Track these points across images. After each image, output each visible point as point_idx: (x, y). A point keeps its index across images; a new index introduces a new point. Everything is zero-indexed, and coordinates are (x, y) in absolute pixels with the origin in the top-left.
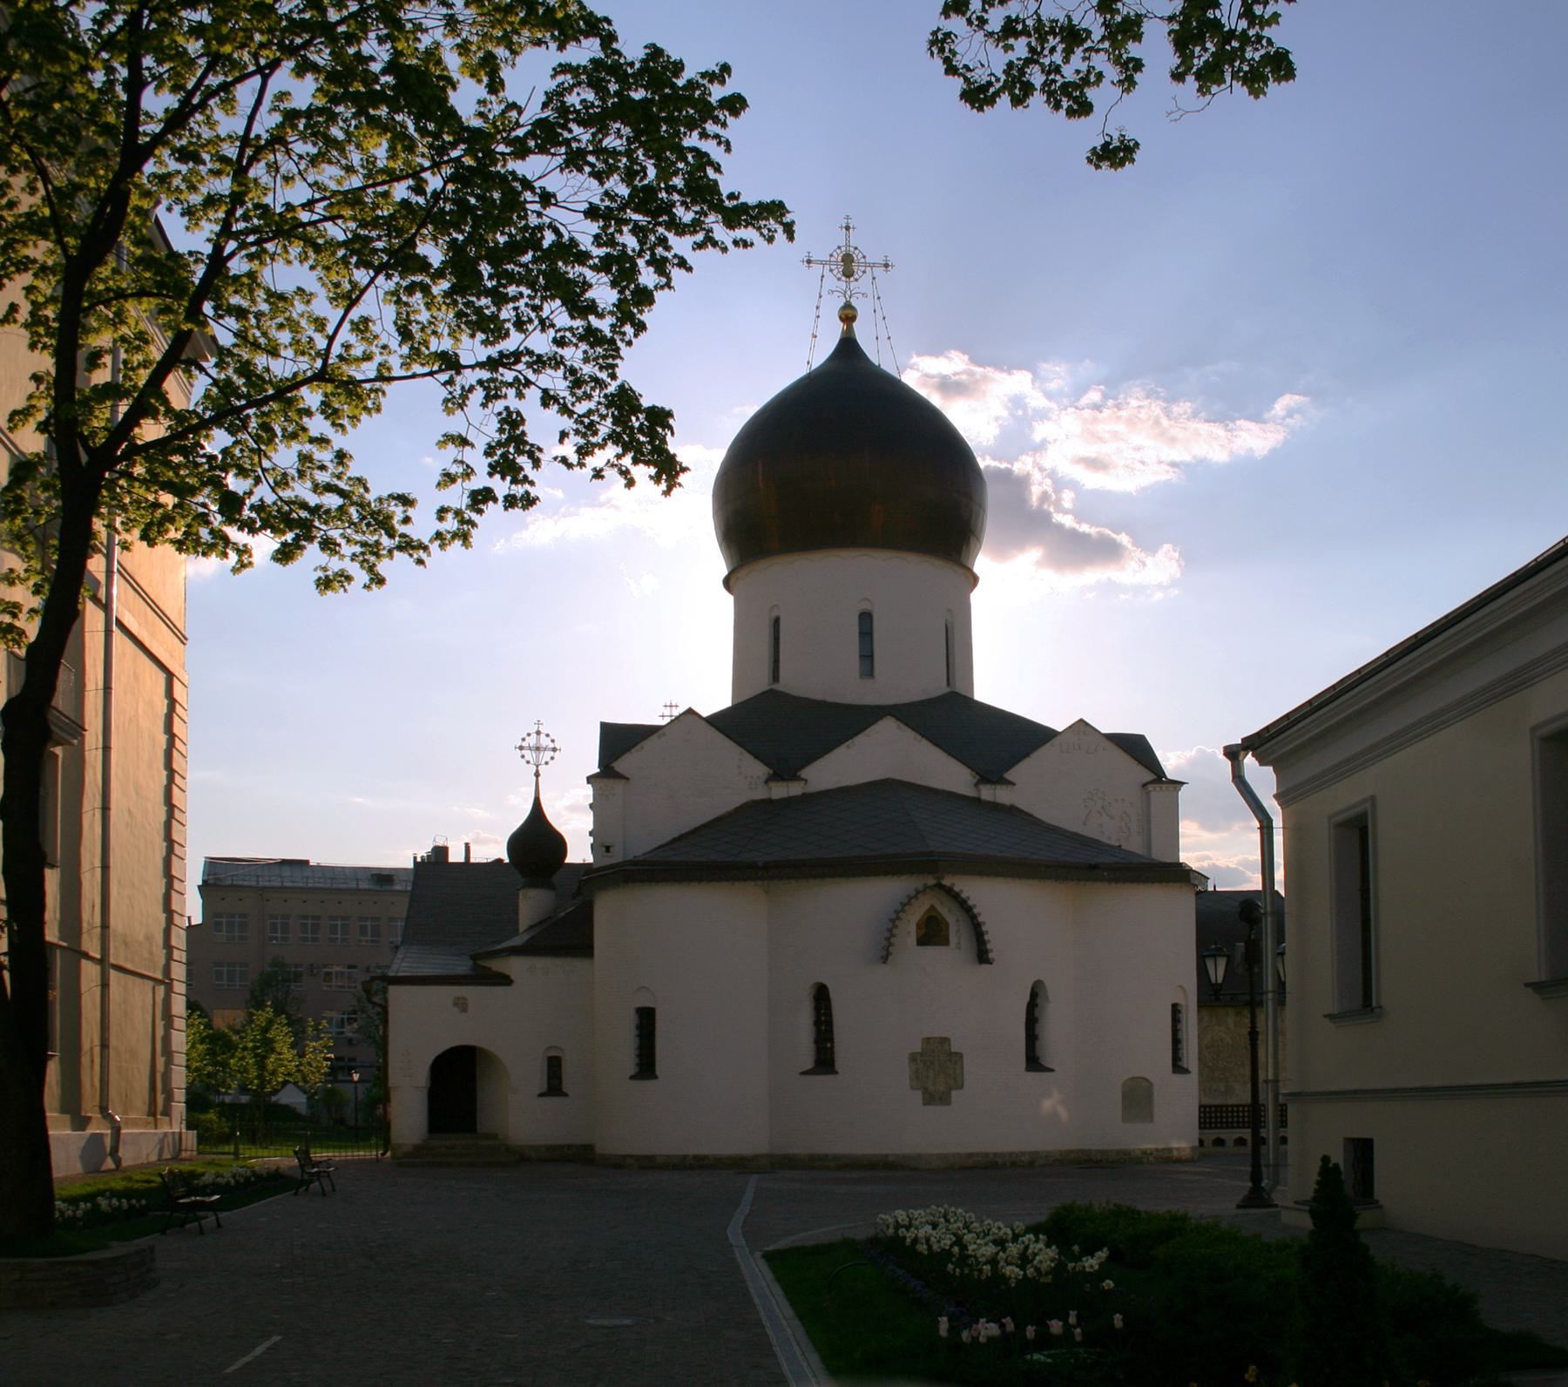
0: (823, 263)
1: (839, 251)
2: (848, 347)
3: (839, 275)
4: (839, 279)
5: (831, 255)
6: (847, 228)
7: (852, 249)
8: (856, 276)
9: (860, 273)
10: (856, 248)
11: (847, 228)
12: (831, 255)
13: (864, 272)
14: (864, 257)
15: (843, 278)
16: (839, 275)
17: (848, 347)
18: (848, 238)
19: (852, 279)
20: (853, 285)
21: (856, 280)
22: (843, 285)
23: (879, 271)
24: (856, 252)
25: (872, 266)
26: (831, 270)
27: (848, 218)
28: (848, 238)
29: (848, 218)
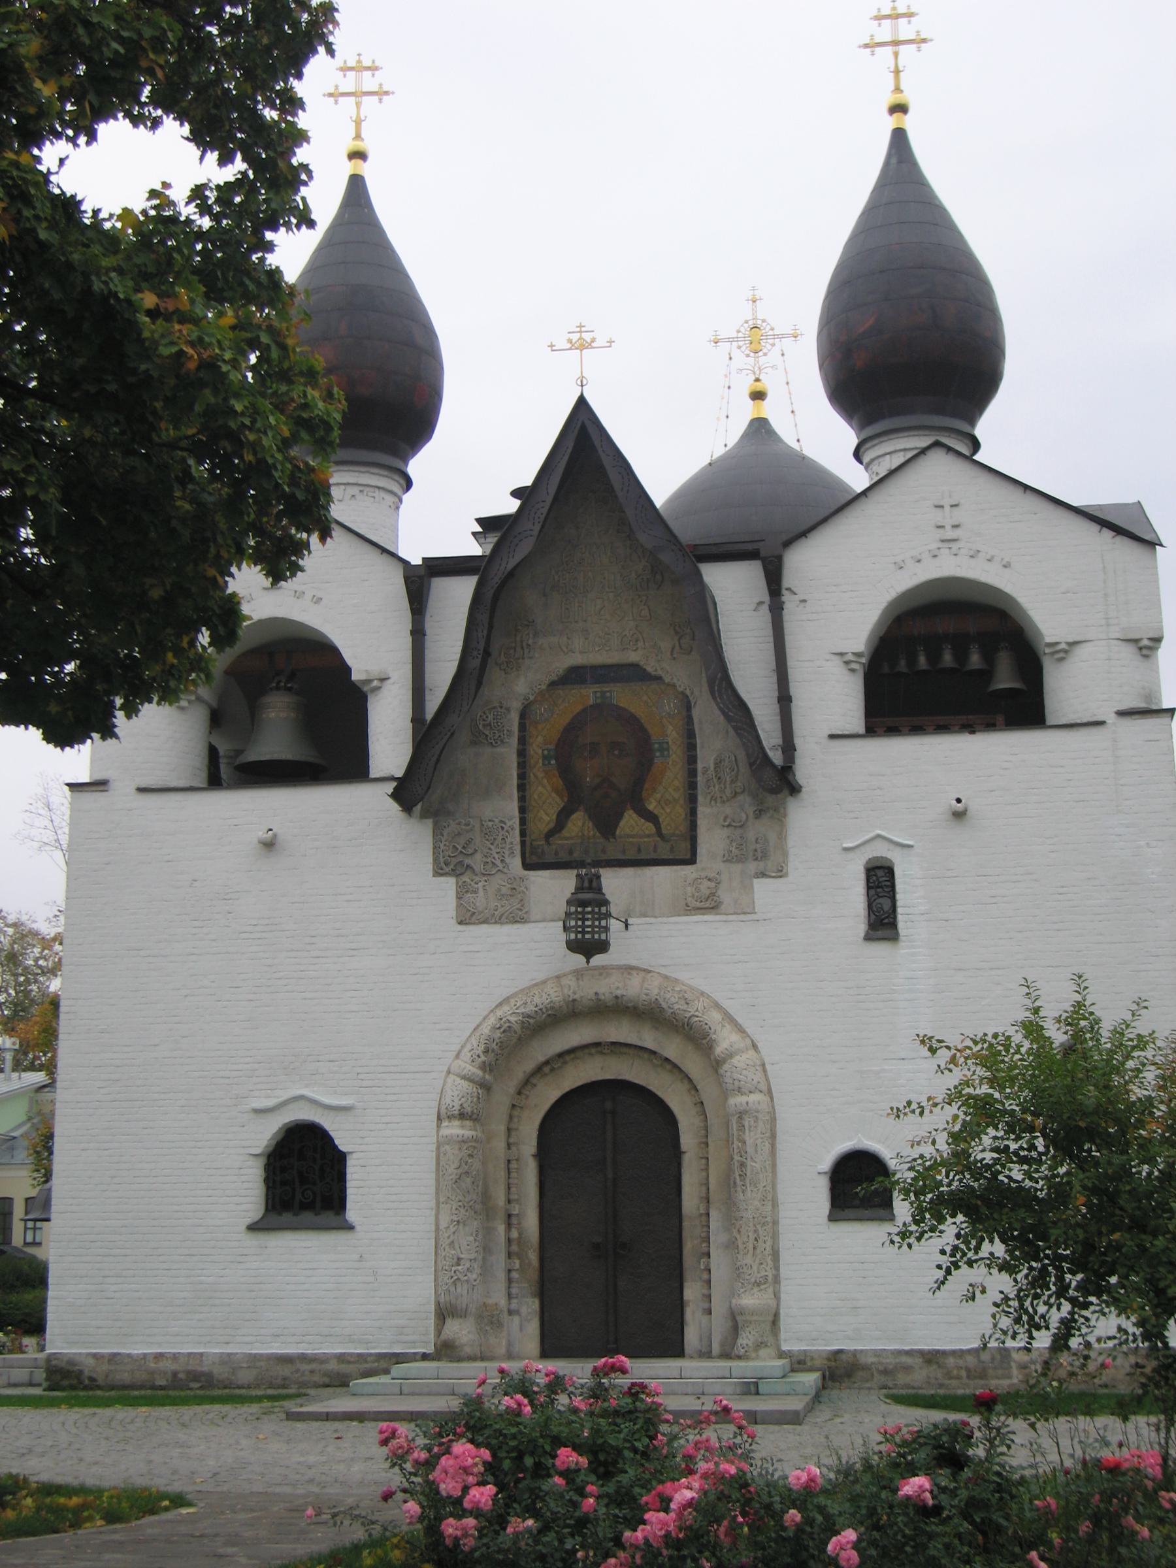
0: (730, 340)
1: (746, 325)
2: (760, 428)
3: (748, 352)
4: (748, 356)
5: (738, 332)
6: (754, 302)
7: (759, 322)
8: (765, 351)
9: (769, 347)
10: (764, 321)
11: (754, 302)
12: (738, 332)
13: (773, 345)
14: (772, 329)
15: (752, 354)
16: (748, 352)
17: (760, 428)
18: (754, 311)
19: (761, 354)
20: (762, 360)
21: (765, 354)
22: (751, 360)
23: (787, 342)
24: (764, 324)
25: (781, 337)
26: (739, 347)
27: (754, 289)
28: (754, 311)
29: (754, 289)
